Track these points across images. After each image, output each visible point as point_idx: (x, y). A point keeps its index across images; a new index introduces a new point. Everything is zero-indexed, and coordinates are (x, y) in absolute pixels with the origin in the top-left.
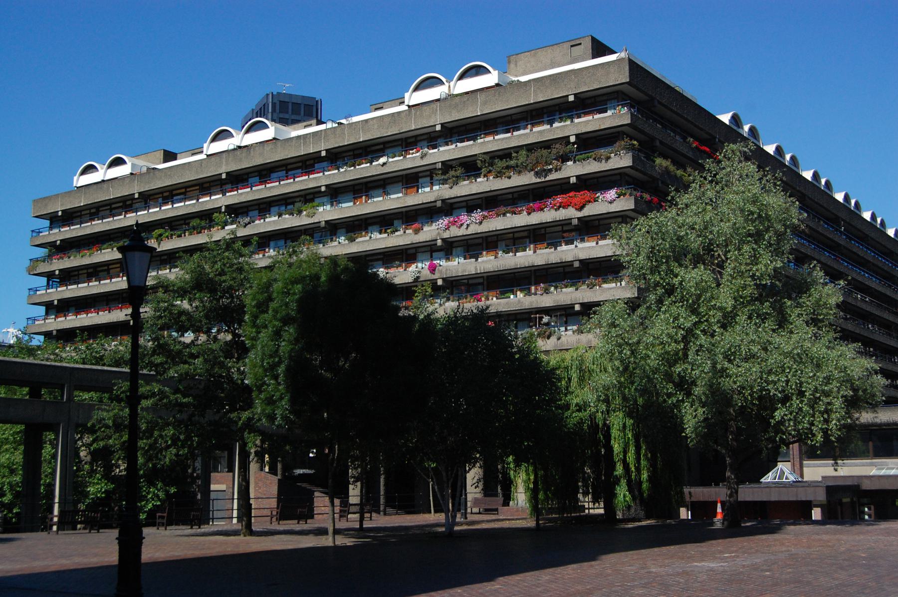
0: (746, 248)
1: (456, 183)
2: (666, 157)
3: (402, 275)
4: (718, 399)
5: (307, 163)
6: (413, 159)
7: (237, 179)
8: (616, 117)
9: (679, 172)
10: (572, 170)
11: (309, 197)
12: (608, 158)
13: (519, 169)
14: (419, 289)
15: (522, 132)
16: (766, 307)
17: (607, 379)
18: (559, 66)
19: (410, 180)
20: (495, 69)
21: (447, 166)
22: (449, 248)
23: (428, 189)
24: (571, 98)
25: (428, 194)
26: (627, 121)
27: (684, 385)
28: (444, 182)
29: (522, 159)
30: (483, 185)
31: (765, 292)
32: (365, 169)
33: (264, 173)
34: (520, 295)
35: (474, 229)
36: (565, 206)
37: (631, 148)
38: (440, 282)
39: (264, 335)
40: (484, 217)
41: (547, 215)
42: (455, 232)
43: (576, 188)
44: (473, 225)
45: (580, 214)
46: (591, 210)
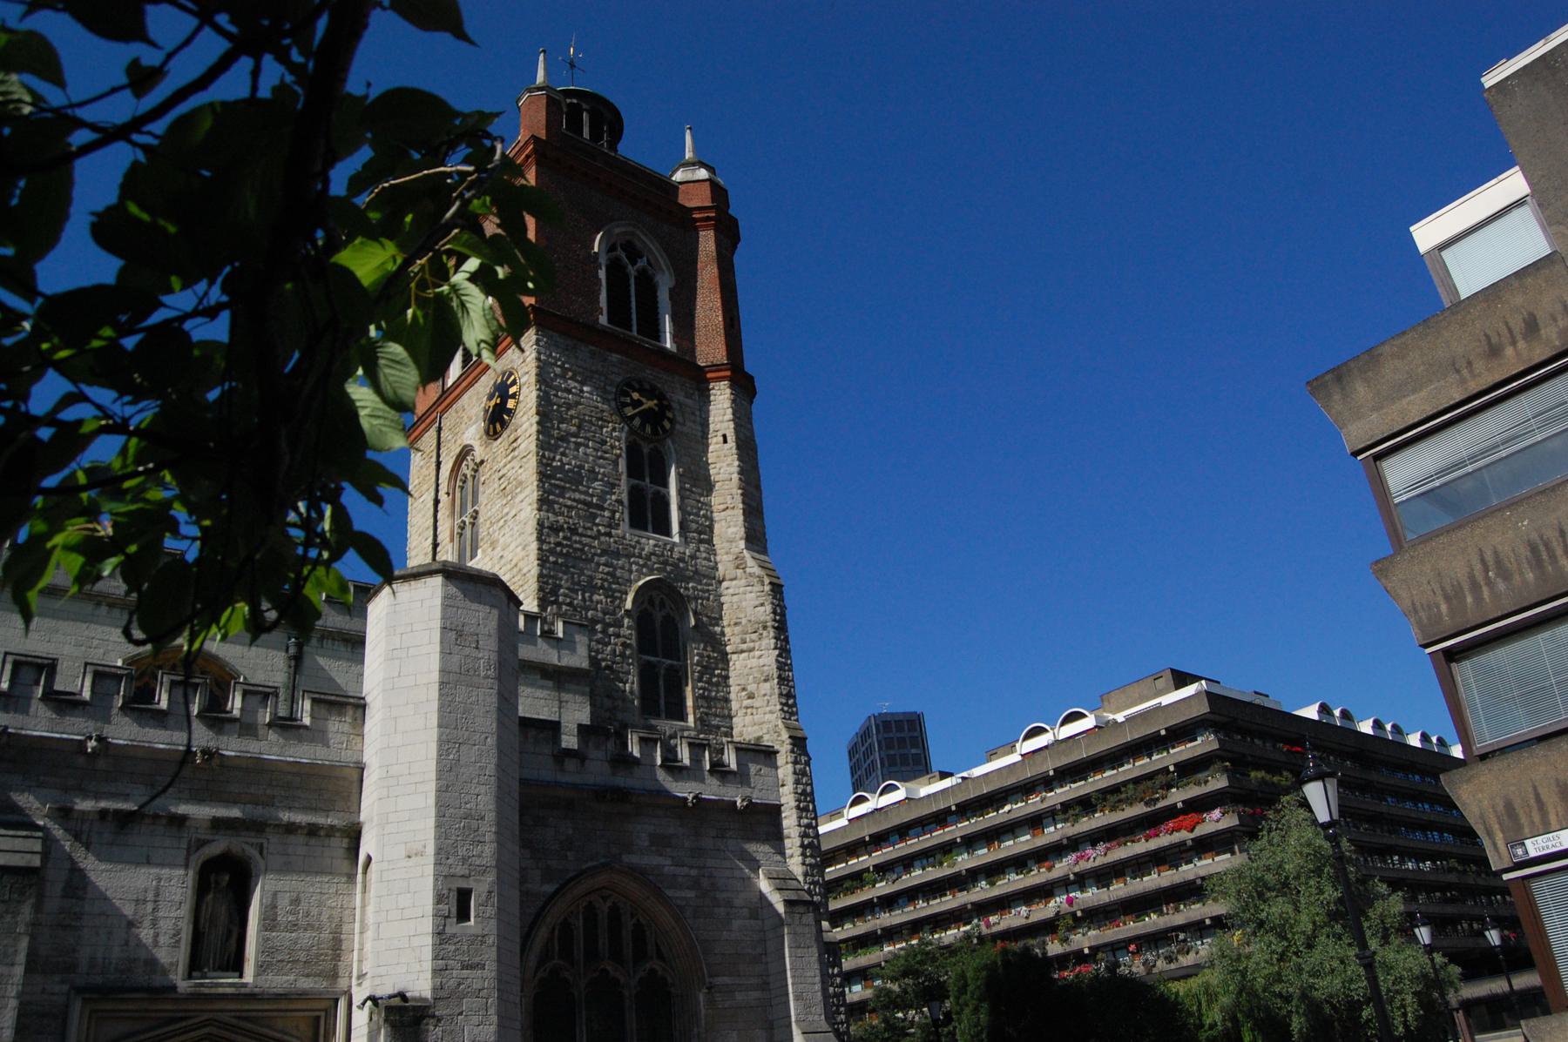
0: (1312, 883)
1: (1076, 821)
2: (1258, 768)
3: (1054, 948)
4: (1313, 1008)
5: (940, 818)
6: (1035, 803)
7: (879, 840)
8: (1205, 743)
9: (1276, 779)
10: (1177, 796)
11: (947, 849)
12: (1206, 782)
13: (1130, 802)
14: (1061, 923)
15: (1127, 767)
16: (1338, 928)
17: (1225, 1000)
18: (1148, 699)
19: (1035, 822)
20: (1091, 711)
21: (1066, 806)
22: (1081, 880)
23: (1052, 829)
24: (1163, 732)
25: (1053, 833)
26: (1216, 746)
27: (1287, 999)
28: (1065, 821)
29: (1130, 793)
30: (1101, 819)
31: (1333, 916)
32: (992, 818)
33: (903, 831)
34: (1154, 916)
35: (1100, 861)
36: (1178, 830)
37: (1226, 770)
38: (1079, 914)
39: (967, 1011)
40: (1108, 849)
41: (1163, 840)
42: (1084, 865)
43: (1184, 812)
44: (1098, 857)
45: (1192, 836)
46: (1200, 831)
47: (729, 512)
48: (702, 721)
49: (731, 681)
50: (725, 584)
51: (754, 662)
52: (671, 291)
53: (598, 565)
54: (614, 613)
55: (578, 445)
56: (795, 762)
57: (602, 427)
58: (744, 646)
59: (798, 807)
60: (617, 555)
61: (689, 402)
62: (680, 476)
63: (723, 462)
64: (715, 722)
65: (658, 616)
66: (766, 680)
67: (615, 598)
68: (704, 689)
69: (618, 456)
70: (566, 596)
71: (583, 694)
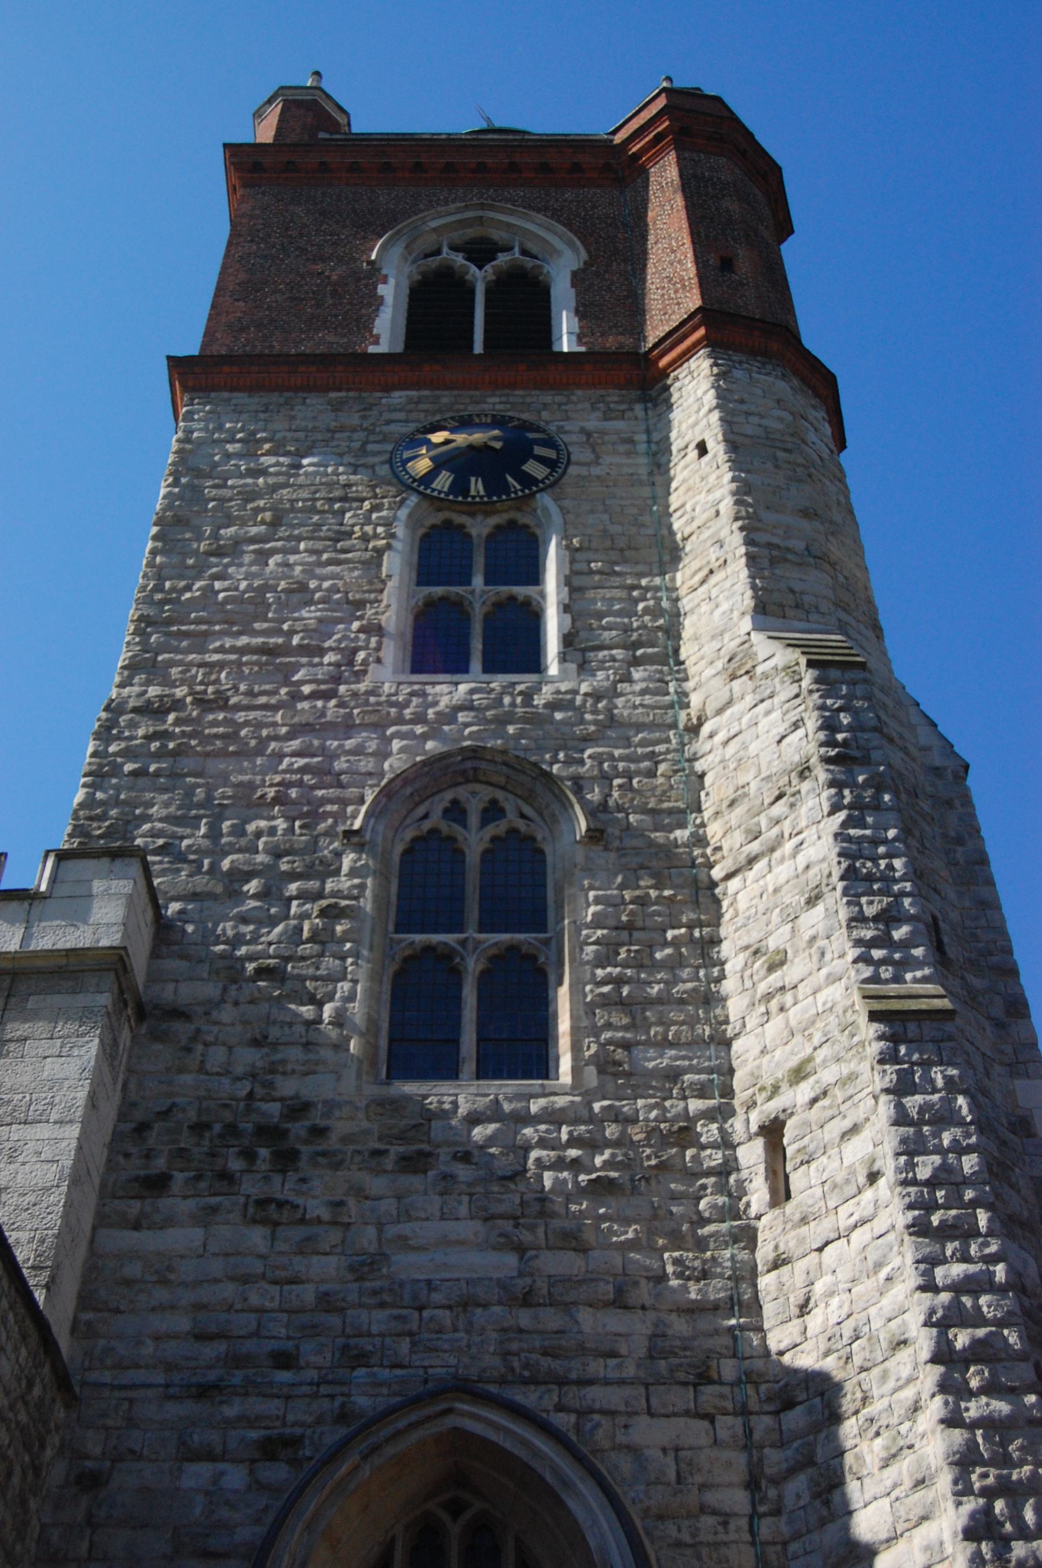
47: (713, 580)
48: (610, 1068)
49: (726, 949)
50: (706, 730)
51: (783, 872)
52: (577, 279)
53: (280, 756)
54: (313, 846)
55: (262, 557)
56: (901, 1089)
57: (342, 512)
58: (755, 847)
59: (919, 1229)
60: (348, 727)
61: (619, 425)
62: (572, 554)
63: (702, 494)
64: (655, 1061)
65: (474, 841)
66: (812, 902)
67: (313, 817)
68: (618, 981)
69: (379, 552)
70: (154, 834)
71: (84, 1015)
